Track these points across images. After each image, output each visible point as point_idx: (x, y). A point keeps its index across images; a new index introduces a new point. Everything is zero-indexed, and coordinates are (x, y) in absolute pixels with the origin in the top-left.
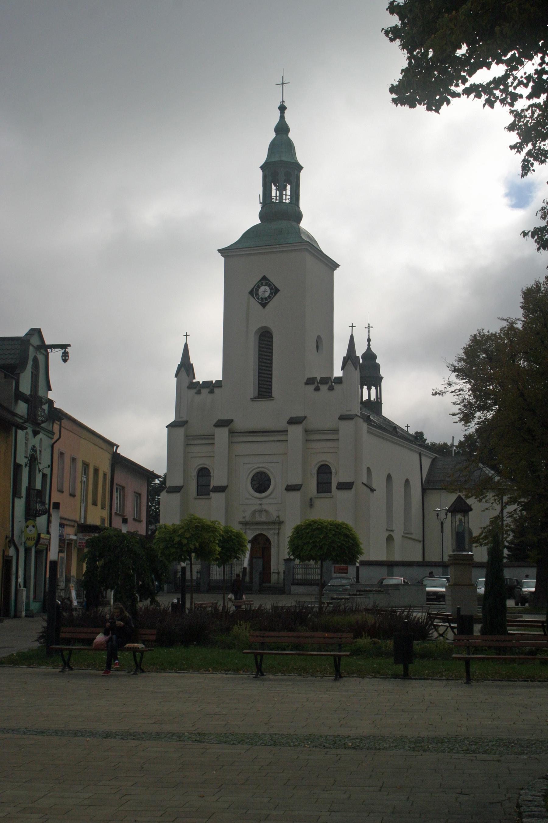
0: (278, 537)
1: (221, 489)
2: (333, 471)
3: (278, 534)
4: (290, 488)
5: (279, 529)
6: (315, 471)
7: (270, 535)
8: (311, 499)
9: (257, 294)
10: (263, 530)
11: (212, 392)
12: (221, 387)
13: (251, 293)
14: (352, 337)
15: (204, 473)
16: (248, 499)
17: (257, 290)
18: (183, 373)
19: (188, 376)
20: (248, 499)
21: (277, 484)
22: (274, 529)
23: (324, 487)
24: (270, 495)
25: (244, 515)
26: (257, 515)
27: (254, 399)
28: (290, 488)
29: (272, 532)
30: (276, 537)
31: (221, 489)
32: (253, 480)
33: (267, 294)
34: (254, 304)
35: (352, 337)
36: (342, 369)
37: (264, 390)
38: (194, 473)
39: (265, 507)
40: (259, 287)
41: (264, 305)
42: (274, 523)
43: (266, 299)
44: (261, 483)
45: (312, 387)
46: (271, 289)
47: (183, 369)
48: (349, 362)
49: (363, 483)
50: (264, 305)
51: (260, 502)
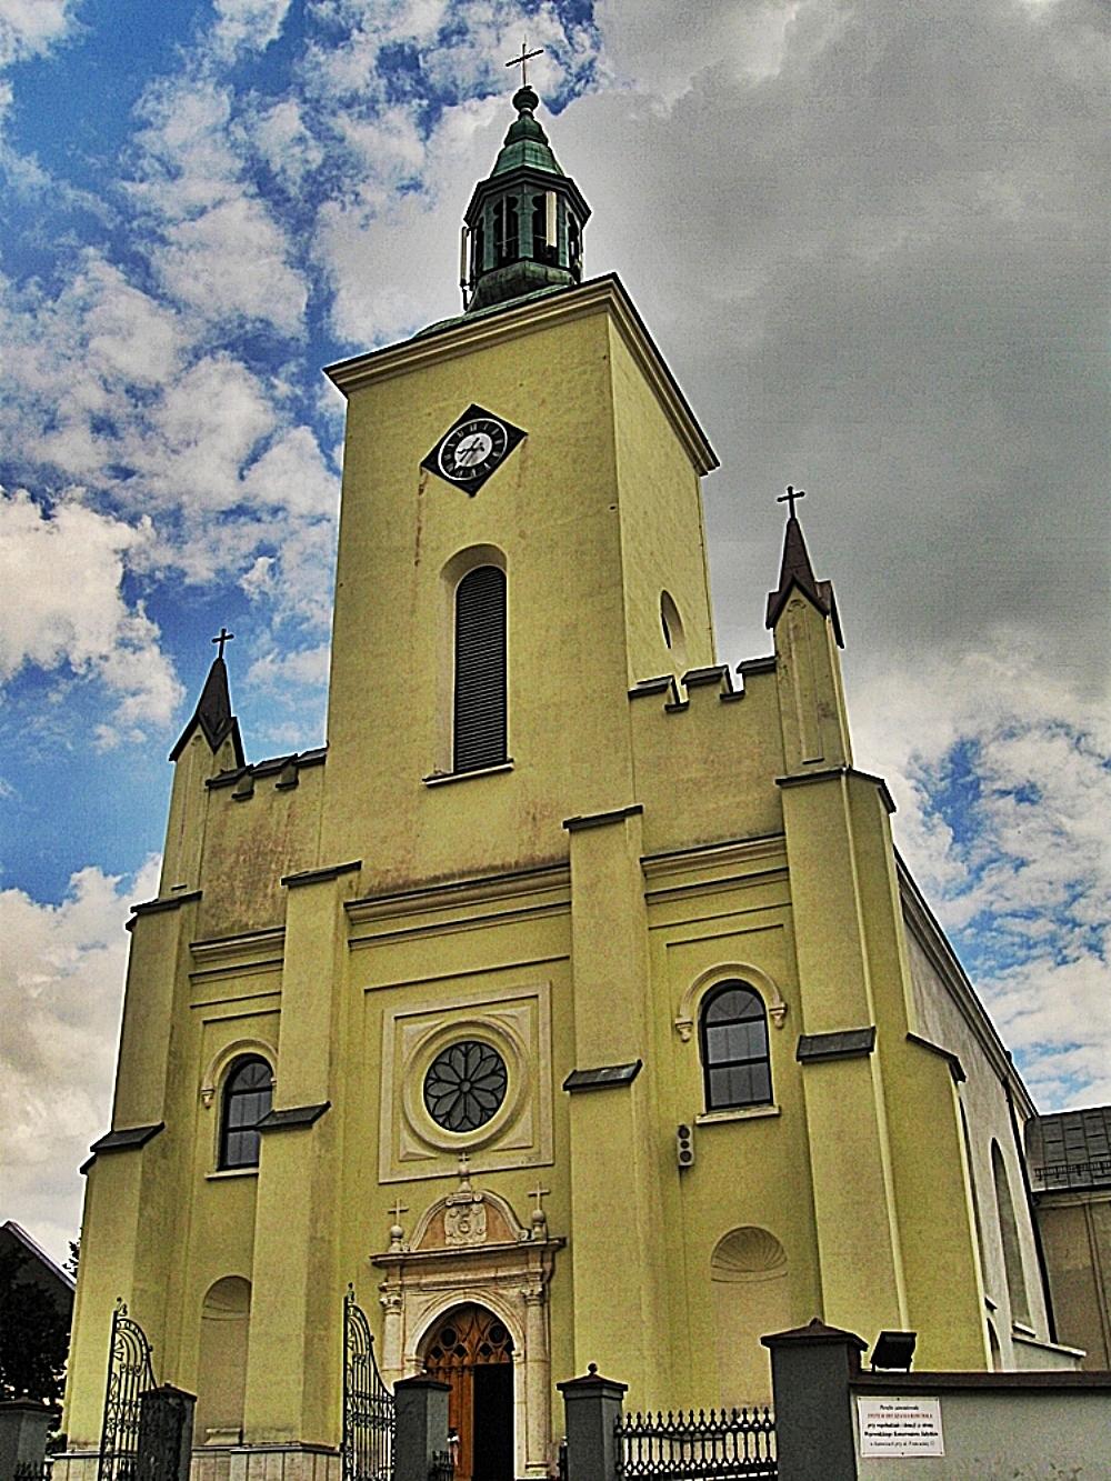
0: (546, 1318)
1: (300, 1121)
2: (772, 1003)
3: (543, 1298)
4: (583, 1085)
5: (546, 1278)
6: (690, 1012)
7: (506, 1305)
8: (683, 1131)
9: (448, 462)
10: (475, 1284)
11: (290, 785)
12: (322, 761)
13: (430, 463)
14: (793, 523)
15: (247, 1073)
16: (410, 1158)
17: (450, 451)
18: (199, 749)
19: (215, 749)
20: (410, 1158)
21: (531, 1076)
22: (525, 1278)
23: (737, 1086)
24: (501, 1133)
25: (396, 1229)
26: (450, 1224)
27: (436, 784)
28: (583, 1085)
29: (513, 1293)
30: (534, 1310)
31: (300, 1121)
32: (432, 1078)
33: (482, 457)
34: (441, 489)
35: (793, 523)
36: (771, 623)
37: (480, 743)
38: (212, 1079)
39: (478, 1186)
40: (456, 440)
41: (471, 487)
42: (520, 1252)
43: (479, 467)
44: (465, 1082)
45: (661, 702)
46: (494, 439)
47: (199, 731)
48: (796, 594)
49: (910, 1037)
50: (471, 487)
51: (463, 1167)
